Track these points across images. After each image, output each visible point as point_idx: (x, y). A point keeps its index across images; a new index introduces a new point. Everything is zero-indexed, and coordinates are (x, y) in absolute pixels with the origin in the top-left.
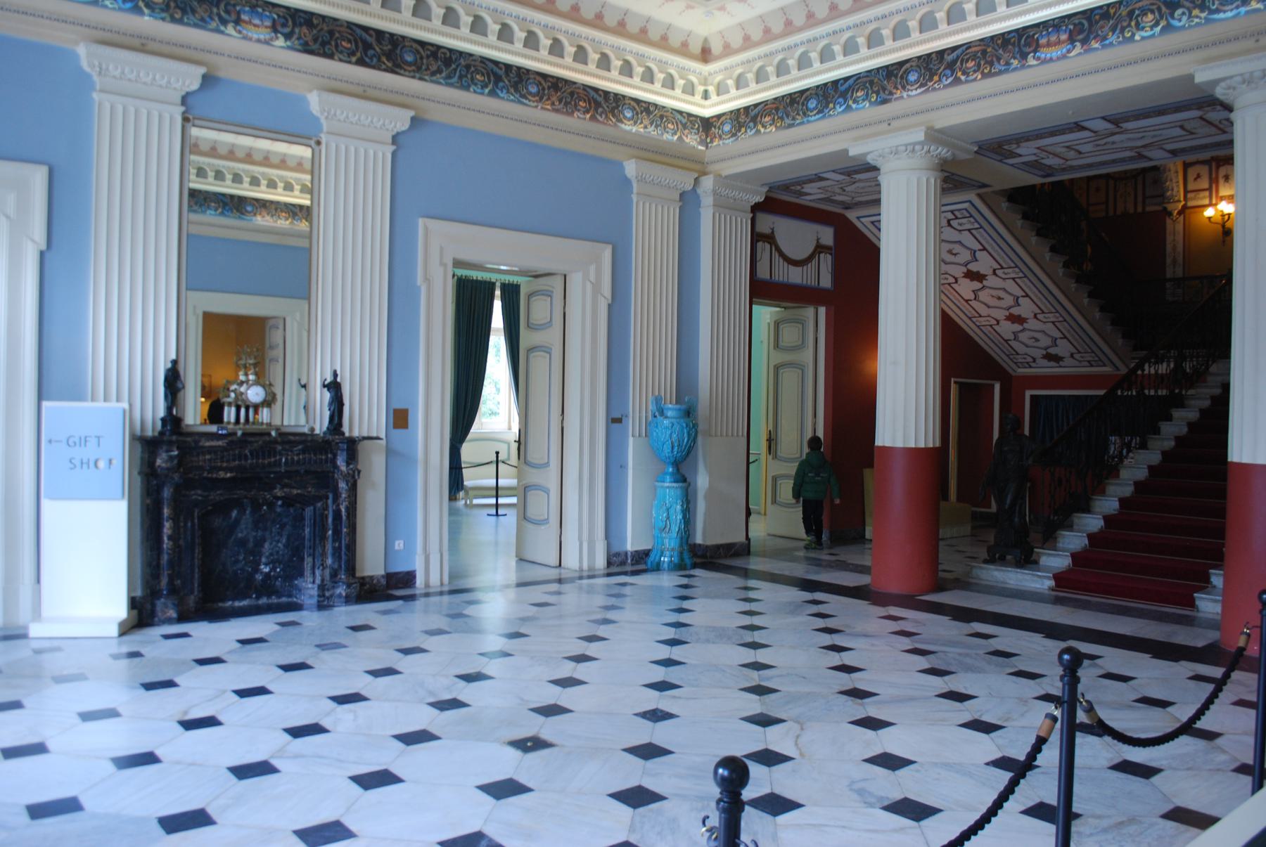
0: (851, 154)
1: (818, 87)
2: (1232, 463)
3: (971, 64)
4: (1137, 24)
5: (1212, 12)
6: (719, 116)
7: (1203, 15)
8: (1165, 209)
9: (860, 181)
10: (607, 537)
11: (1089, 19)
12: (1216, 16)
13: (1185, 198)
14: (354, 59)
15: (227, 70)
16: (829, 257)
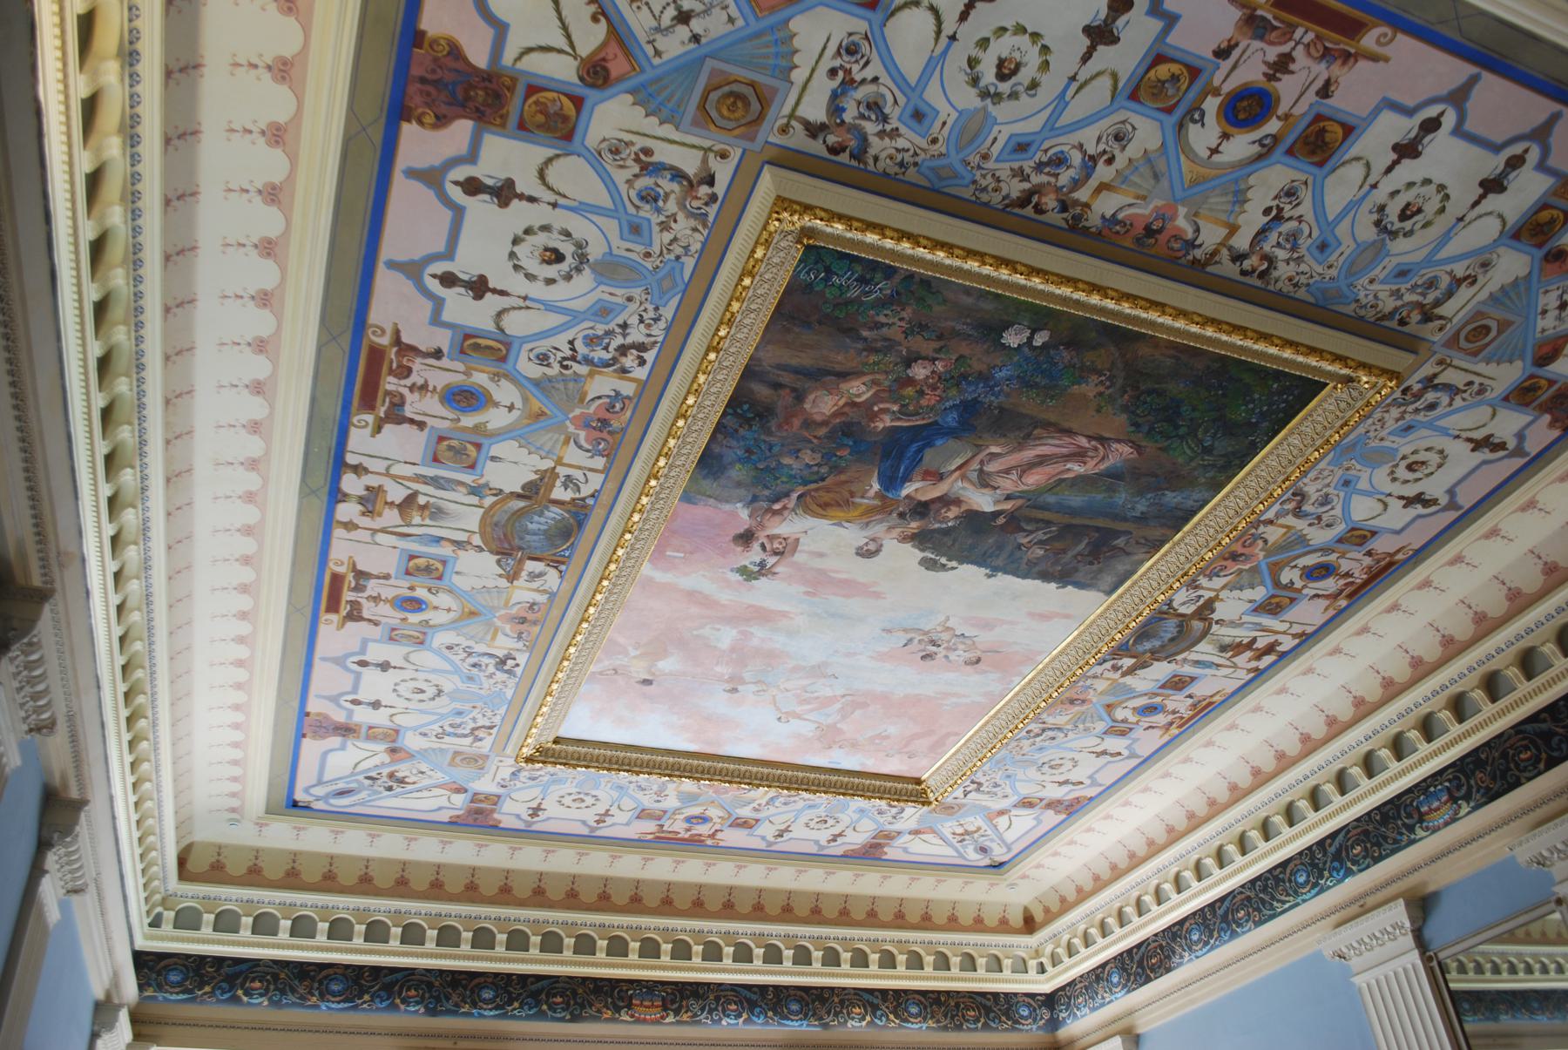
14: (1542, 766)
15: (1436, 878)
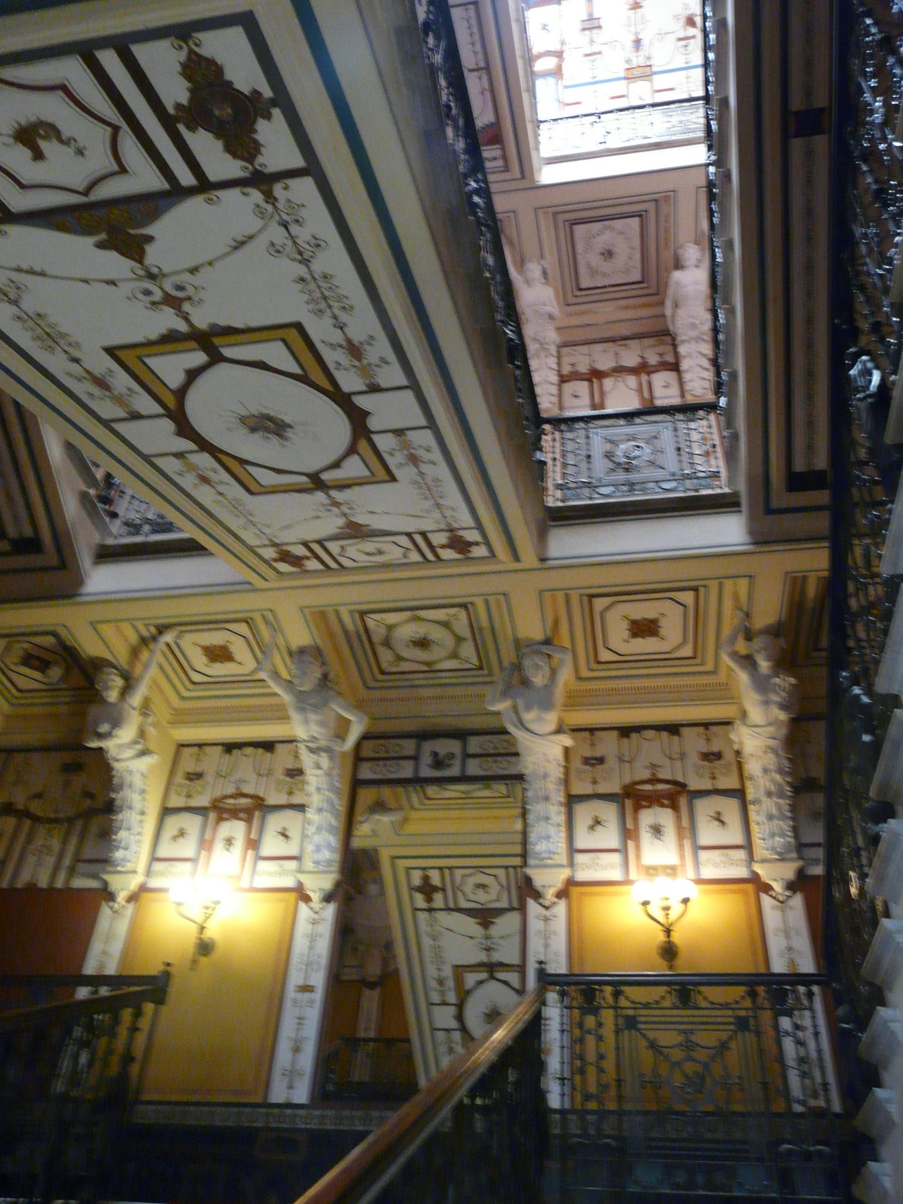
8: (106, 883)
13: (149, 873)
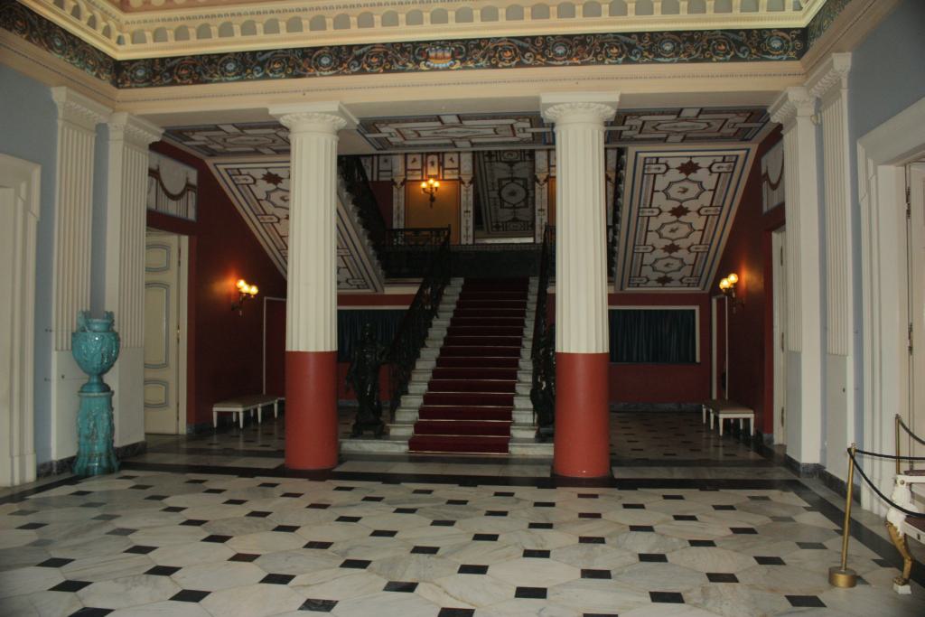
0: (271, 112)
1: (236, 53)
2: (562, 354)
3: (374, 60)
4: (500, 57)
5: (549, 59)
6: (132, 62)
7: (543, 60)
8: (393, 180)
9: (248, 135)
10: (36, 451)
11: (466, 46)
12: (551, 62)
13: (406, 175)
16: (194, 194)
